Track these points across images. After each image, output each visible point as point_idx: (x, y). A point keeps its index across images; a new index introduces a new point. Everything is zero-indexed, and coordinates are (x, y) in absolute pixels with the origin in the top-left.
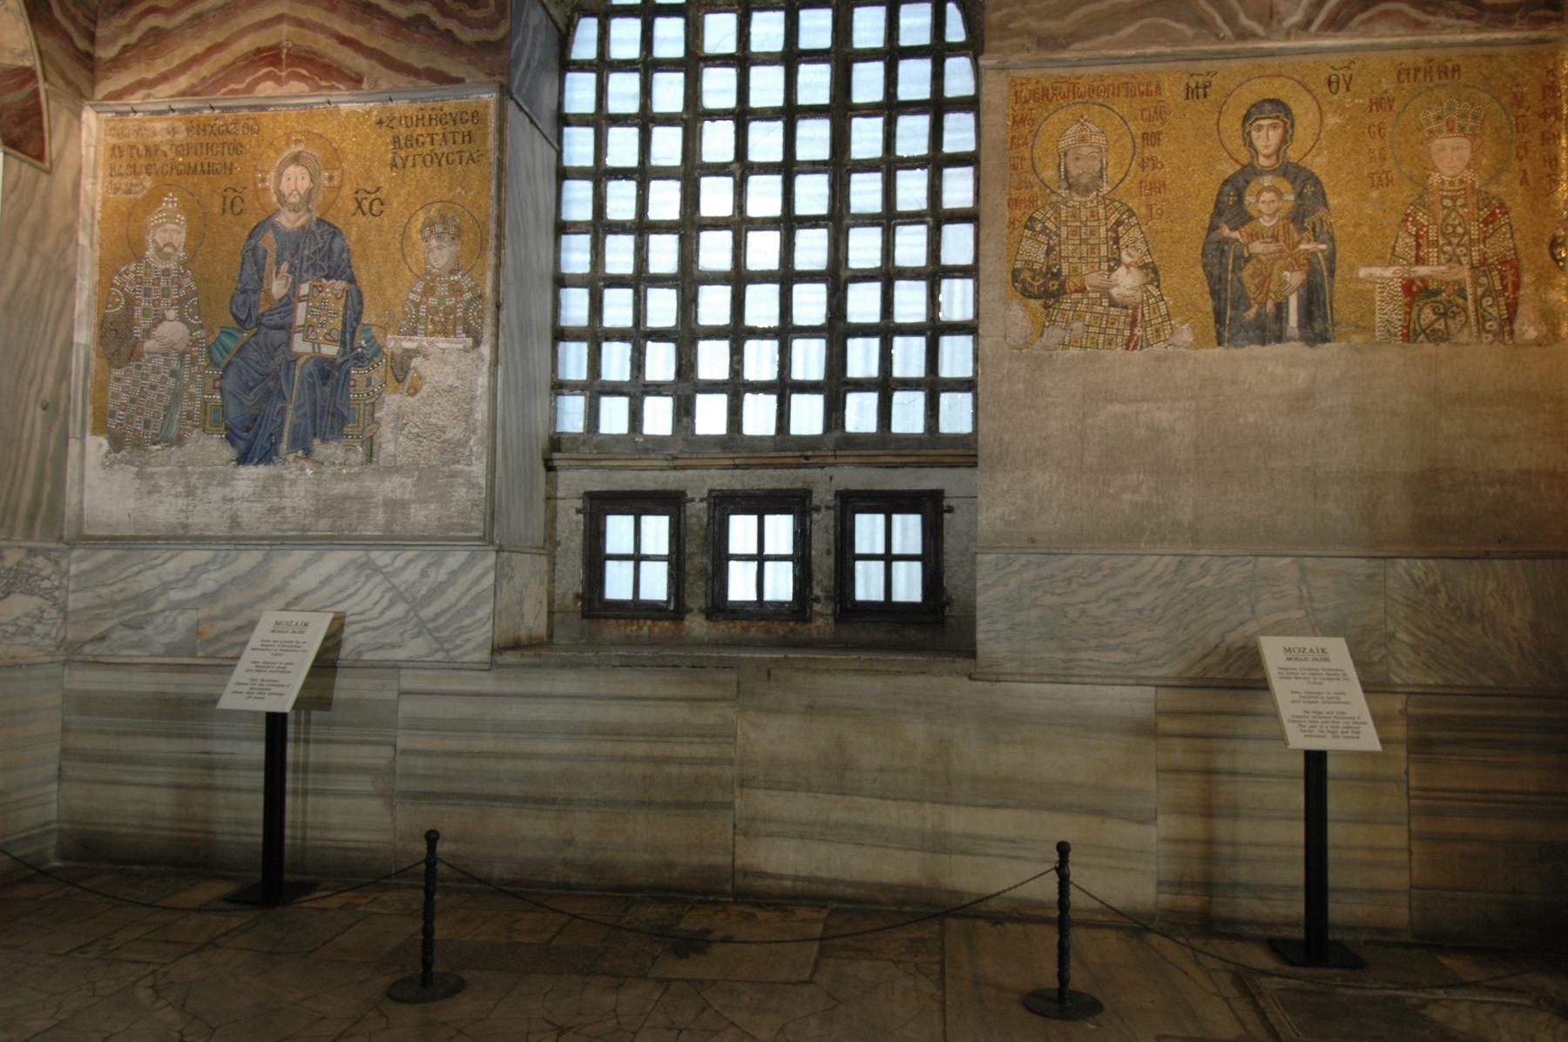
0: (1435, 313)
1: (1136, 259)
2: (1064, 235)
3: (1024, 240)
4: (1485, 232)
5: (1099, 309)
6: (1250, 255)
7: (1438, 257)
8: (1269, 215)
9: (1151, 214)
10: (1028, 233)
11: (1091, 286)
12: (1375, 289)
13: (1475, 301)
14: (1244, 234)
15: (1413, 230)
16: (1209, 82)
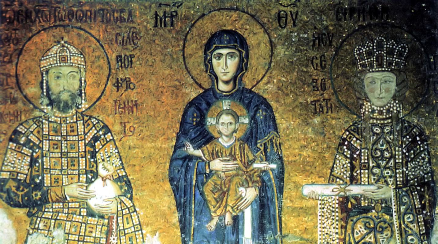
0: (366, 228)
1: (110, 173)
2: (46, 148)
3: (9, 152)
4: (408, 157)
5: (80, 219)
6: (211, 171)
7: (368, 178)
8: (227, 136)
9: (125, 132)
10: (13, 145)
11: (70, 197)
12: (317, 205)
13: (399, 218)
14: (206, 152)
15: (348, 153)
16: (176, 12)
